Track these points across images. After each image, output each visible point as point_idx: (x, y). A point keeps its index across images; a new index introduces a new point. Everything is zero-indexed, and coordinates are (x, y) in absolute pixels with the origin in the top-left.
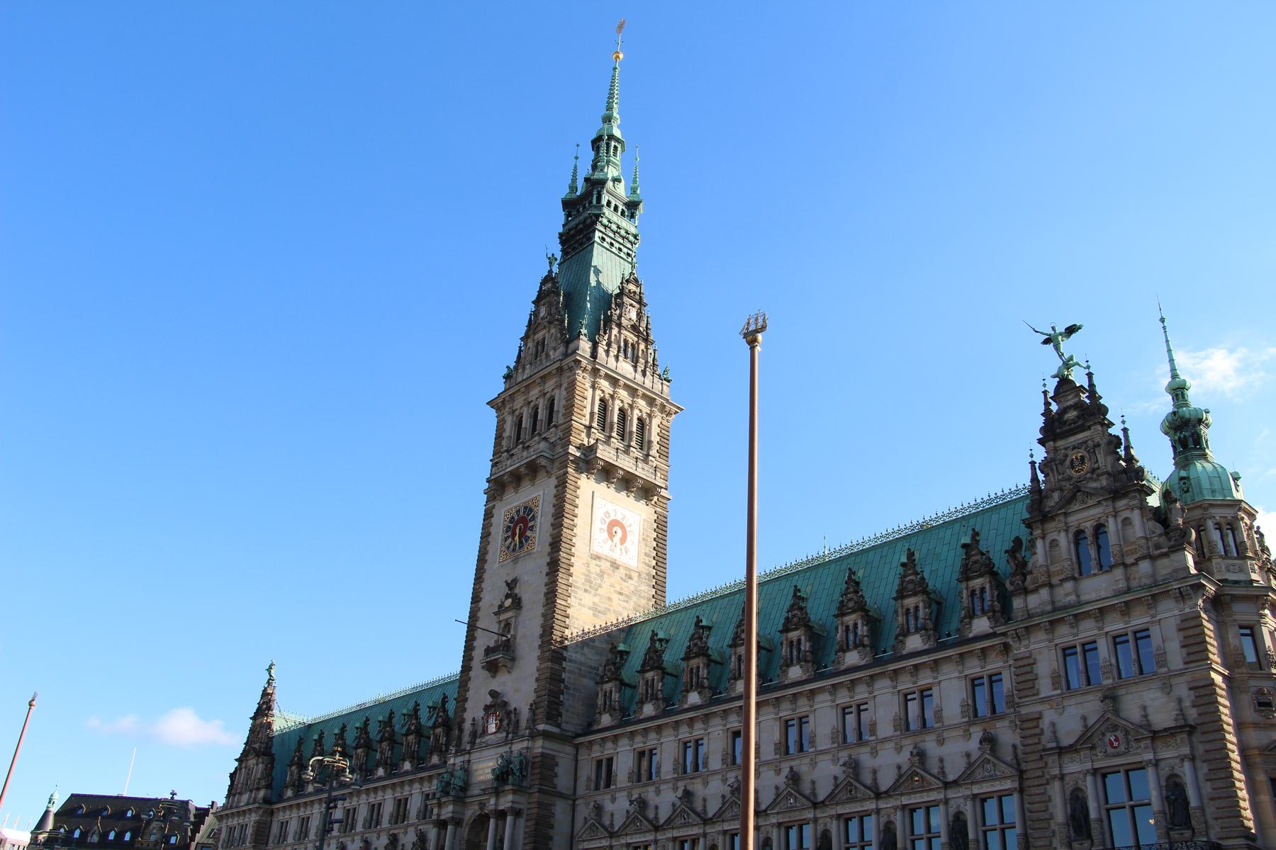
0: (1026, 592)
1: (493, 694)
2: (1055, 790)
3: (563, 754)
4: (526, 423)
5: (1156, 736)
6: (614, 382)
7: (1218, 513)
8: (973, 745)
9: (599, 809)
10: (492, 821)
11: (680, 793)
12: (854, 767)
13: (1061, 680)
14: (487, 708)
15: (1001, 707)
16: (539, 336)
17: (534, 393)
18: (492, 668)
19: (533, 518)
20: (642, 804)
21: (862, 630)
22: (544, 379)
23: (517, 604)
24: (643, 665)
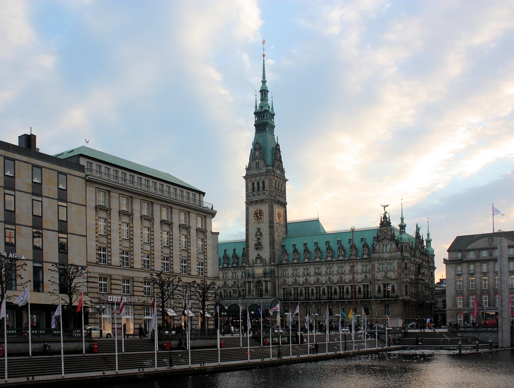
0: (374, 253)
1: (258, 255)
2: (377, 286)
3: (276, 268)
4: (256, 186)
5: (392, 279)
6: (277, 177)
7: (405, 244)
8: (363, 276)
9: (285, 280)
10: (264, 283)
11: (305, 278)
12: (341, 277)
13: (378, 269)
14: (256, 258)
15: (368, 271)
16: (257, 161)
17: (258, 178)
18: (257, 249)
19: (262, 213)
20: (296, 280)
21: (343, 253)
22: (261, 175)
23: (261, 234)
24: (294, 251)
